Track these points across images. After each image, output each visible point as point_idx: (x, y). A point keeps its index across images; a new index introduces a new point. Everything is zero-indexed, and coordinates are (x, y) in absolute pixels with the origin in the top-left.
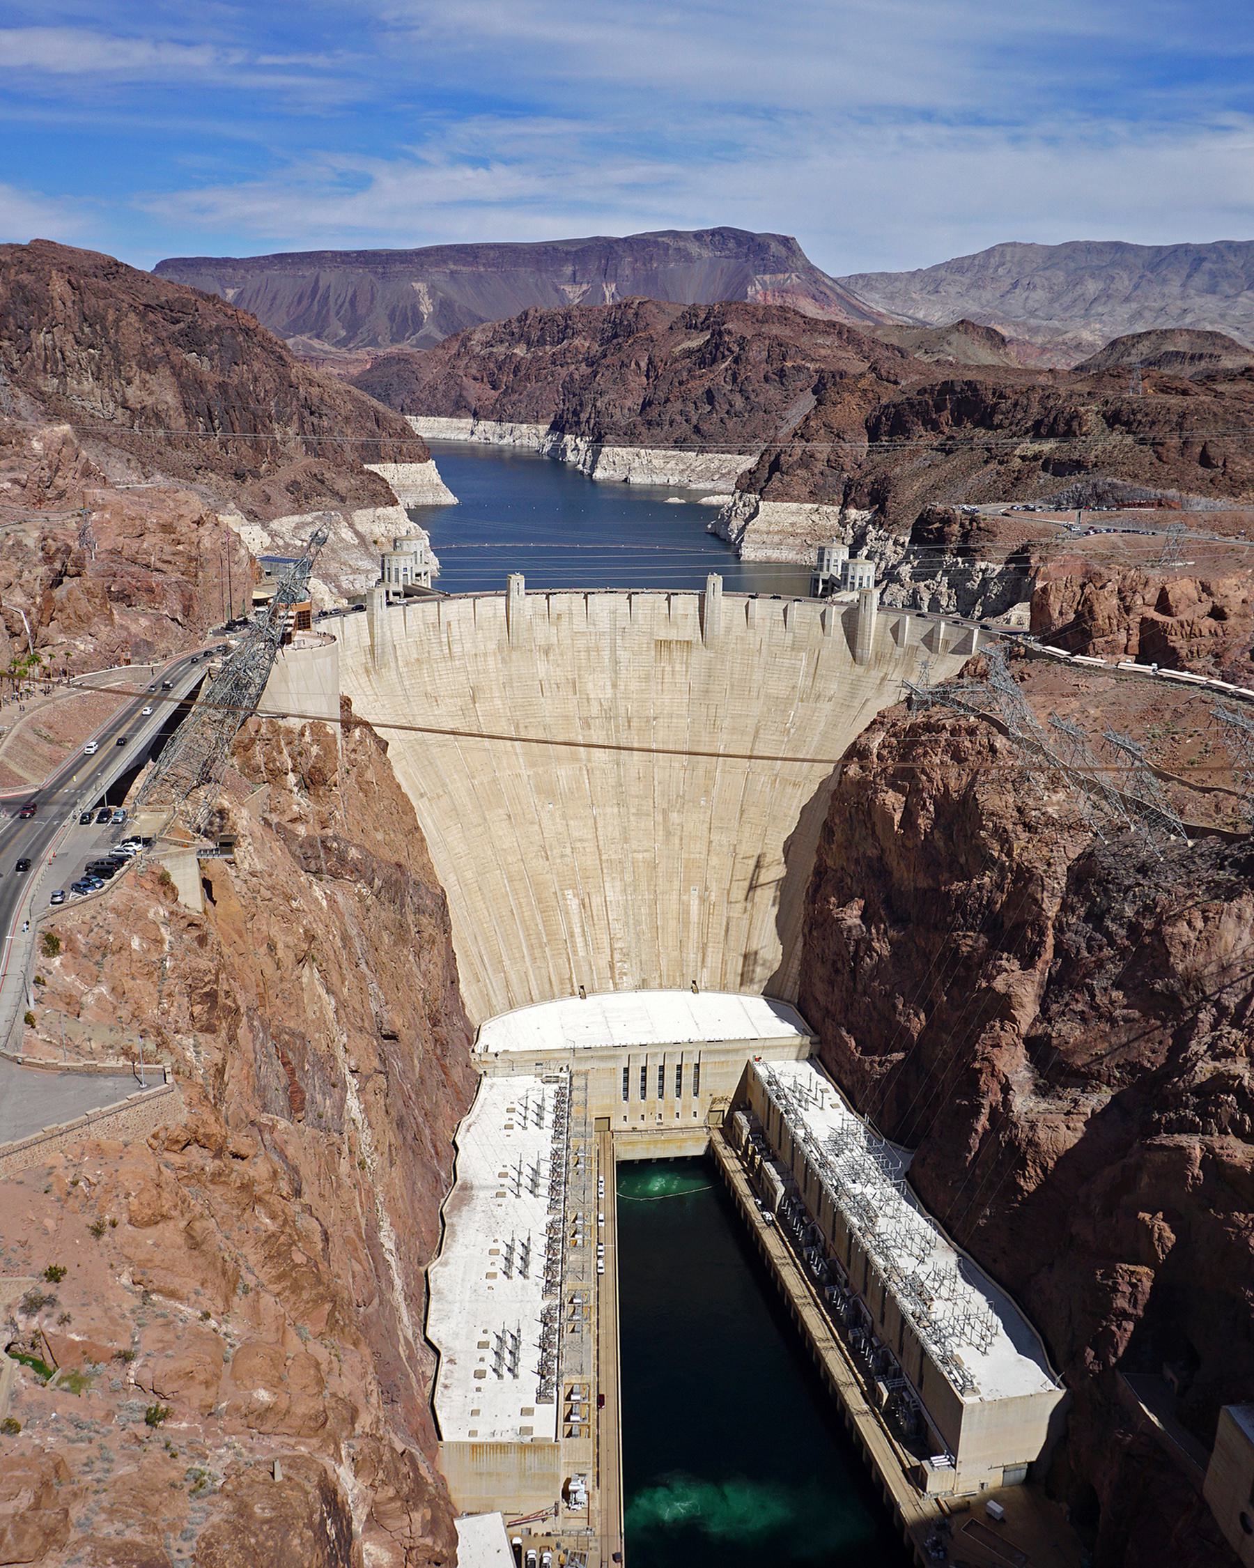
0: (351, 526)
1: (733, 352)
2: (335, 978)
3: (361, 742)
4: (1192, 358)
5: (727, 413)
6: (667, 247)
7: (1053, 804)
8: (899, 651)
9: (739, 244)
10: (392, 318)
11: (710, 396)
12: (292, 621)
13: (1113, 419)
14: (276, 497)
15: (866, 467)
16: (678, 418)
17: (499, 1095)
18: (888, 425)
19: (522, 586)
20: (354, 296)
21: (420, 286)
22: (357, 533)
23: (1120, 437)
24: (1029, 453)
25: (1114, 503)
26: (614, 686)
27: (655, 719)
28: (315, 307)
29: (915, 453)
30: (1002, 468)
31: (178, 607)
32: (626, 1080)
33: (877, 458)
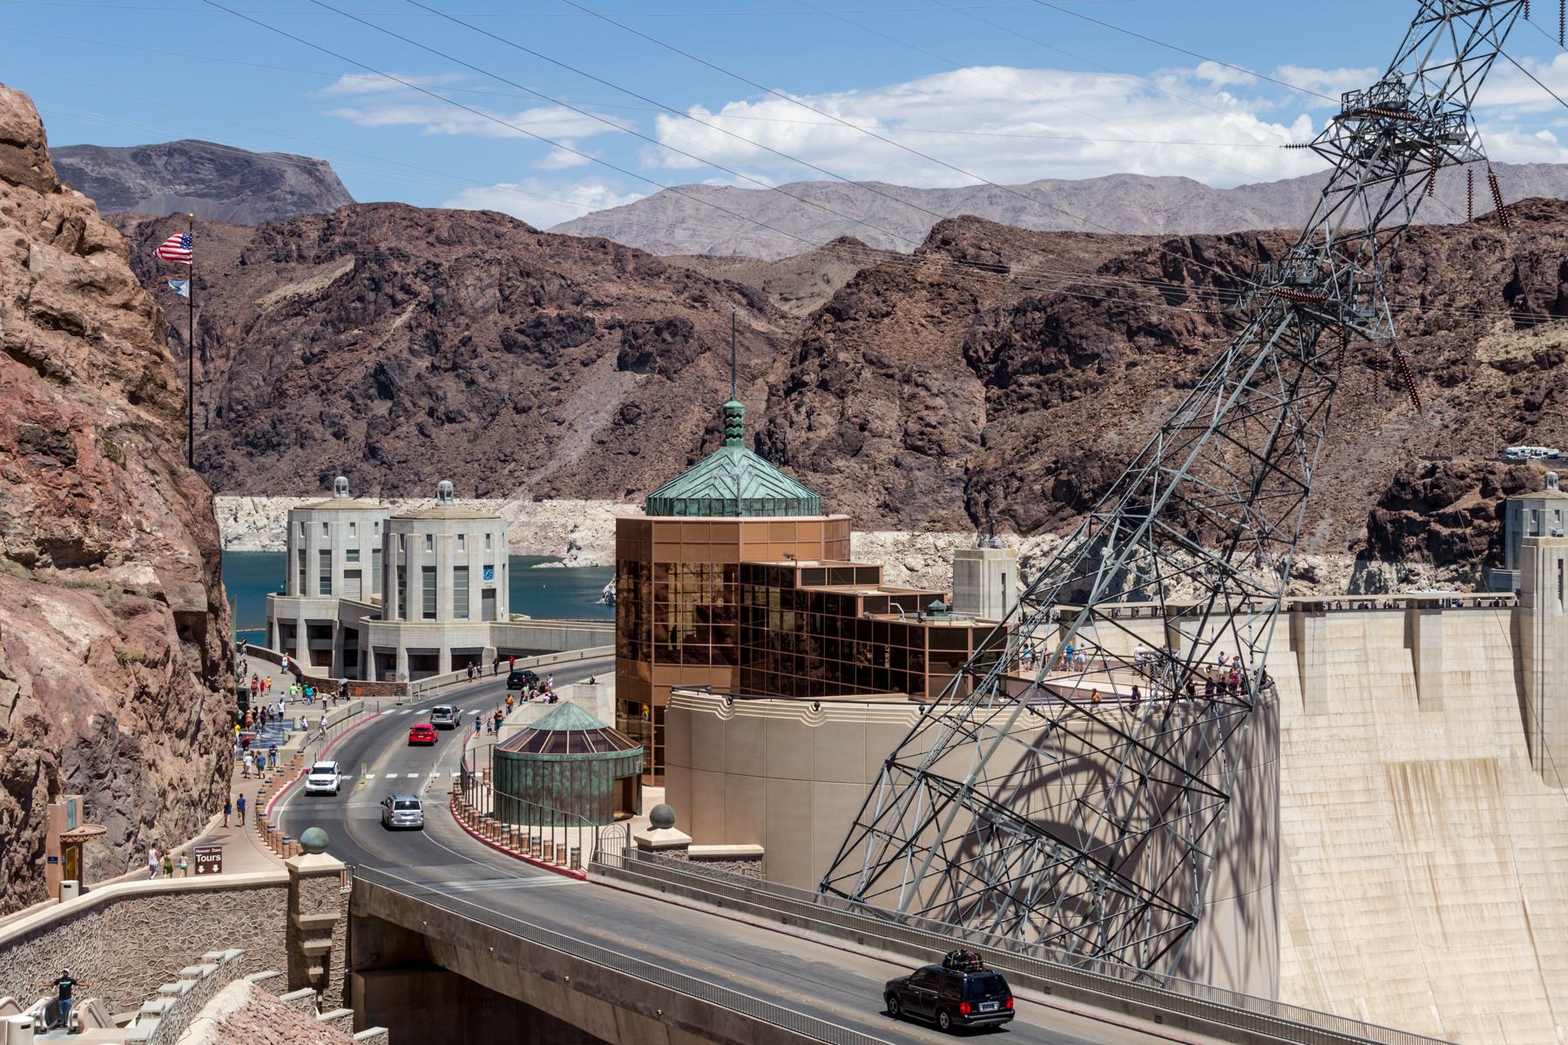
1: (416, 295)
5: (431, 412)
11: (382, 382)
15: (1010, 444)
29: (1138, 397)
30: (1459, 390)
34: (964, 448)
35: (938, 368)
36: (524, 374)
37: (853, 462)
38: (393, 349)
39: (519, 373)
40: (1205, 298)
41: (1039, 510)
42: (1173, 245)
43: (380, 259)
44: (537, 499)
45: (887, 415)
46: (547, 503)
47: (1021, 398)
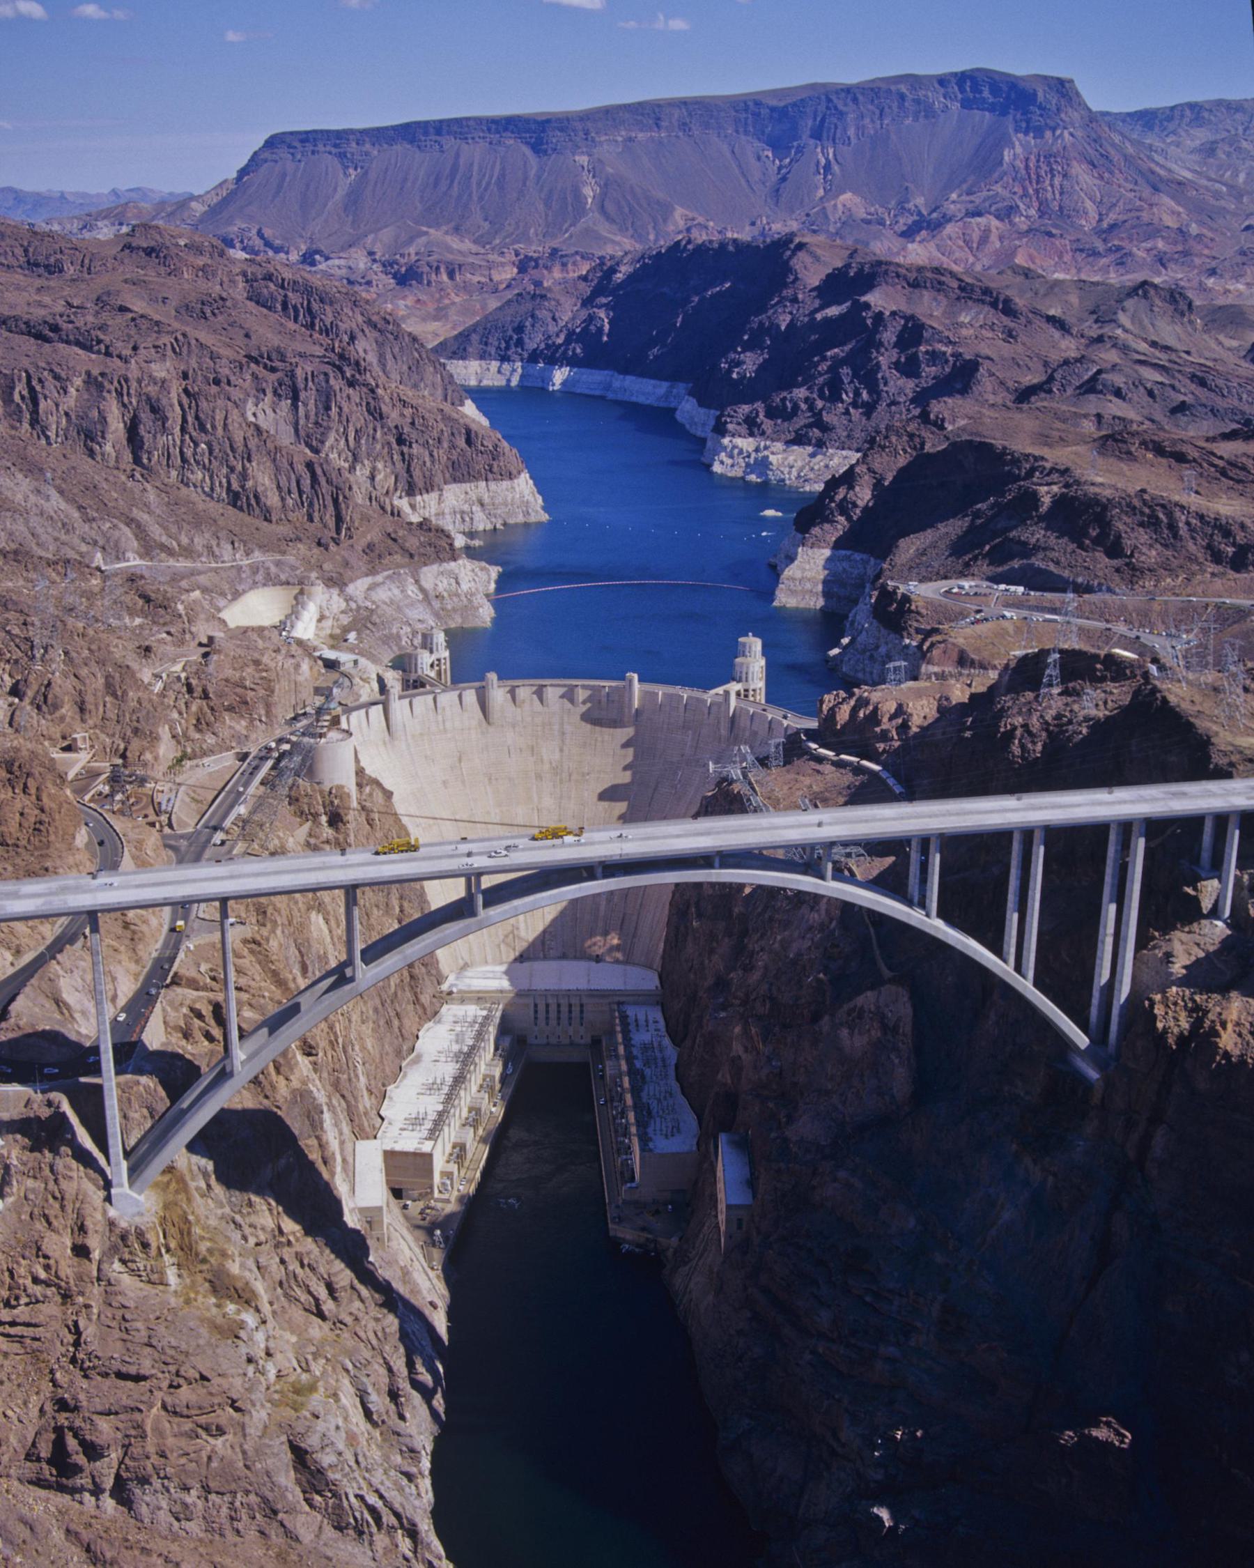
0: (417, 582)
2: (333, 923)
3: (371, 795)
6: (902, 97)
9: (995, 90)
10: (547, 202)
12: (326, 724)
14: (353, 561)
16: (803, 406)
17: (450, 1011)
20: (503, 175)
21: (583, 160)
22: (422, 590)
26: (561, 750)
28: (455, 191)
31: (263, 712)
32: (536, 1012)
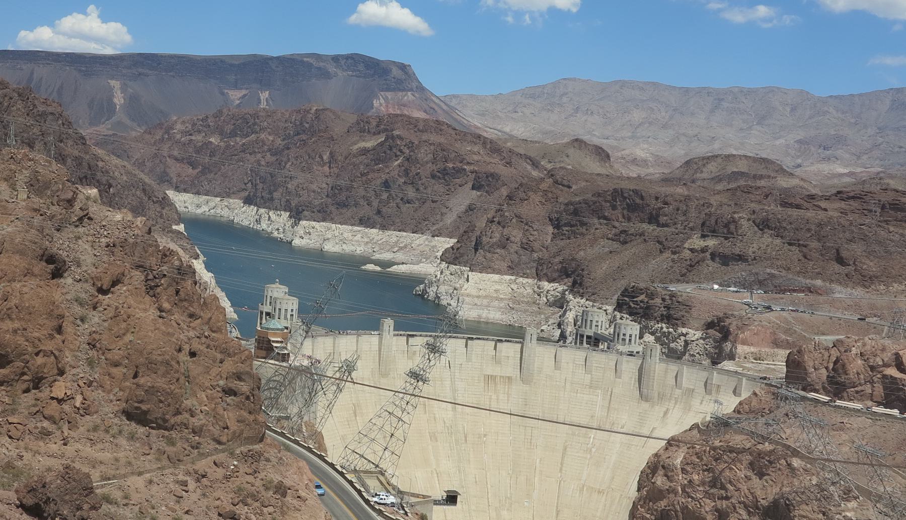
4: (755, 177)
5: (402, 199)
7: (849, 510)
8: (678, 392)
11: (386, 185)
13: (764, 225)
15: (554, 250)
16: (362, 202)
18: (571, 219)
19: (392, 328)
23: (770, 240)
24: (696, 247)
25: (772, 288)
27: (485, 436)
30: (676, 257)
33: (562, 243)
34: (541, 250)
35: (538, 221)
36: (439, 188)
37: (503, 251)
38: (392, 174)
39: (436, 187)
40: (623, 209)
41: (556, 275)
42: (615, 190)
43: (393, 138)
44: (433, 236)
45: (517, 235)
46: (436, 238)
47: (563, 235)
